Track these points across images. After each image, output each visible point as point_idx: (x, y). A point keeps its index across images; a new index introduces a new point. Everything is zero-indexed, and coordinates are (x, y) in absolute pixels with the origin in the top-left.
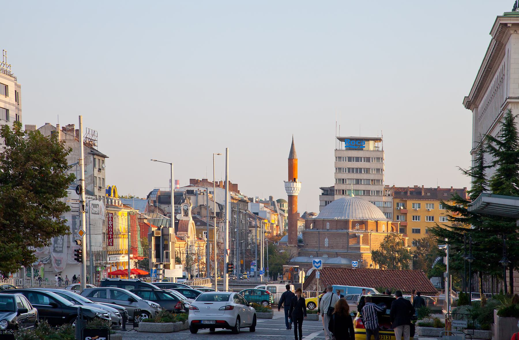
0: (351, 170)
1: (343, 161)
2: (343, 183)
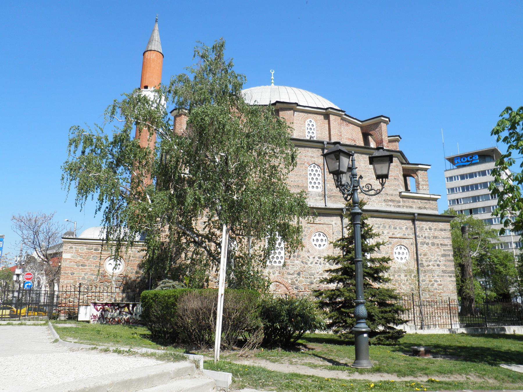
0: (465, 188)
1: (455, 180)
2: (458, 203)
